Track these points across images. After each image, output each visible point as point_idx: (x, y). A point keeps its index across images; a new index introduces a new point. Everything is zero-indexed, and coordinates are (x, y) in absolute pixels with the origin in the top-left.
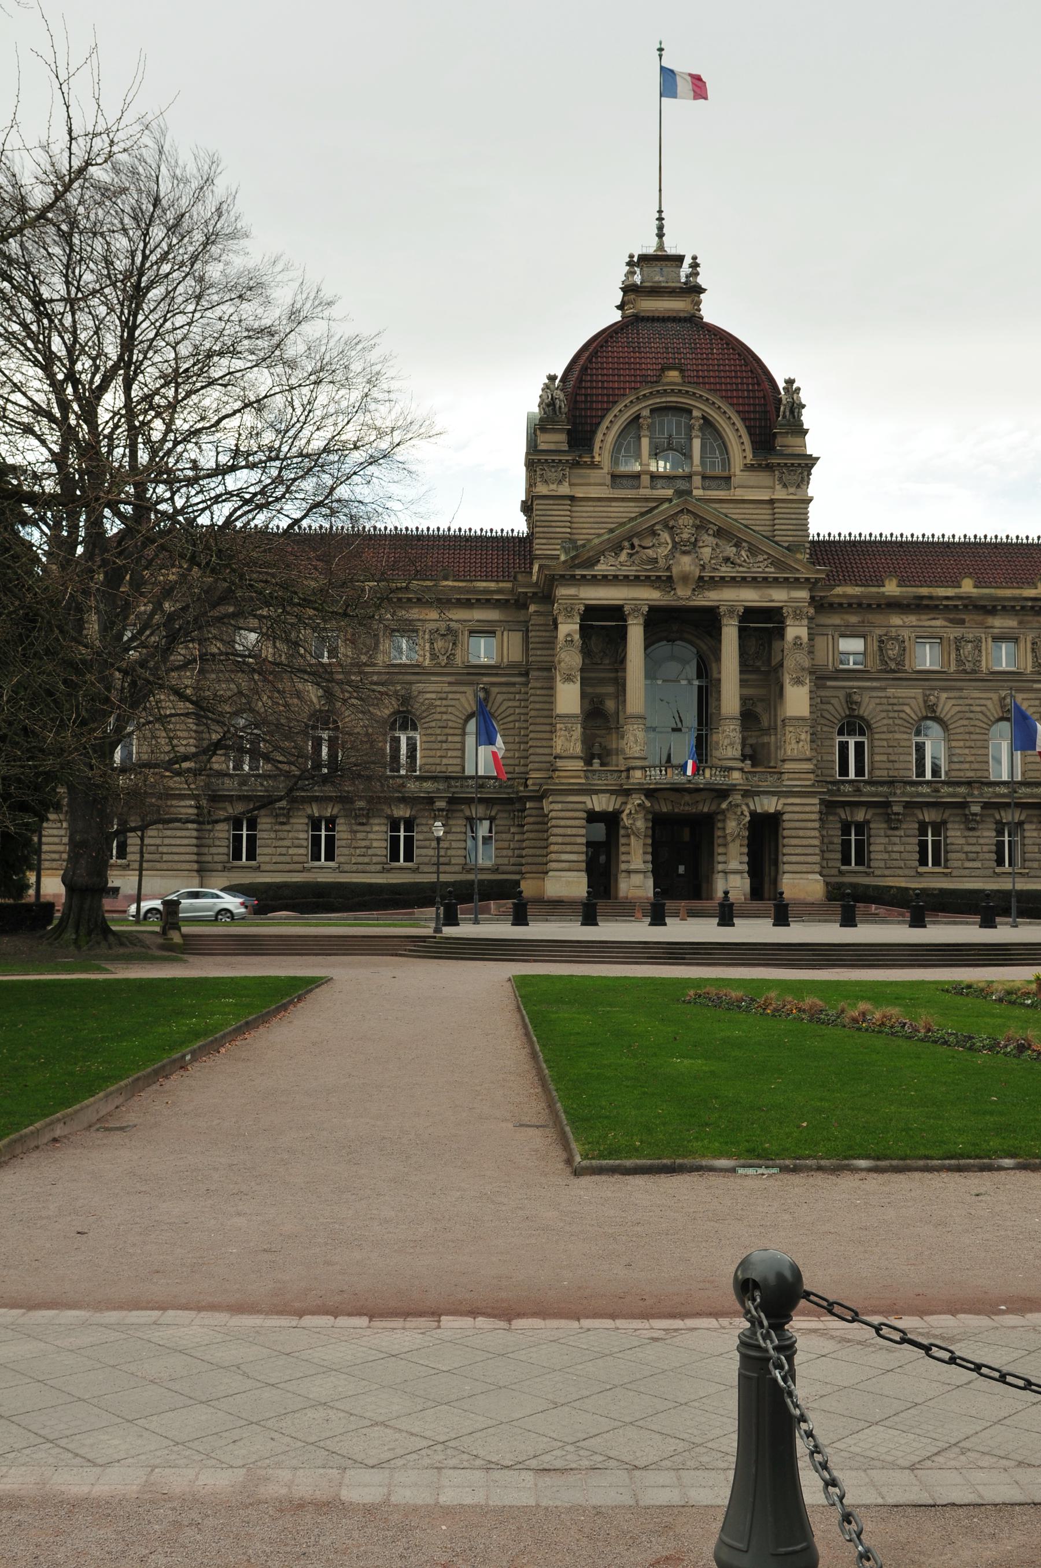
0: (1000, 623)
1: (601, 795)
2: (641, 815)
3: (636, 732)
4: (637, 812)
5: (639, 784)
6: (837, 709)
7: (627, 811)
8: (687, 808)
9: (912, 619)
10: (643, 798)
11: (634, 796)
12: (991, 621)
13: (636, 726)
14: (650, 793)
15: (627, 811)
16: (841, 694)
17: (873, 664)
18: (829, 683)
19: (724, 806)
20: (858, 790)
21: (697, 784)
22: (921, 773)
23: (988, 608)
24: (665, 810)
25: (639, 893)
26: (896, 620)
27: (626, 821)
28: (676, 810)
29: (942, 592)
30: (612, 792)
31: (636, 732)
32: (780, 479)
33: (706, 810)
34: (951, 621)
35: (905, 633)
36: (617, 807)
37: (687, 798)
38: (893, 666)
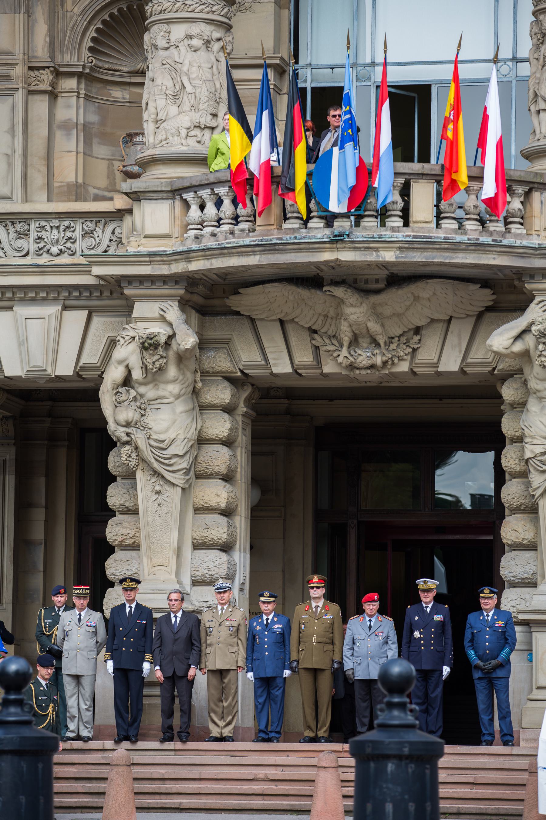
1: (22, 311)
2: (172, 386)
3: (183, 55)
4: (154, 375)
5: (153, 257)
7: (114, 374)
8: (364, 357)
10: (173, 313)
11: (141, 309)
13: (178, 31)
14: (212, 298)
15: (114, 374)
19: (501, 339)
21: (368, 245)
24: (282, 366)
27: (115, 413)
28: (328, 368)
30: (68, 297)
31: (183, 55)
33: (451, 363)
36: (92, 357)
37: (356, 311)
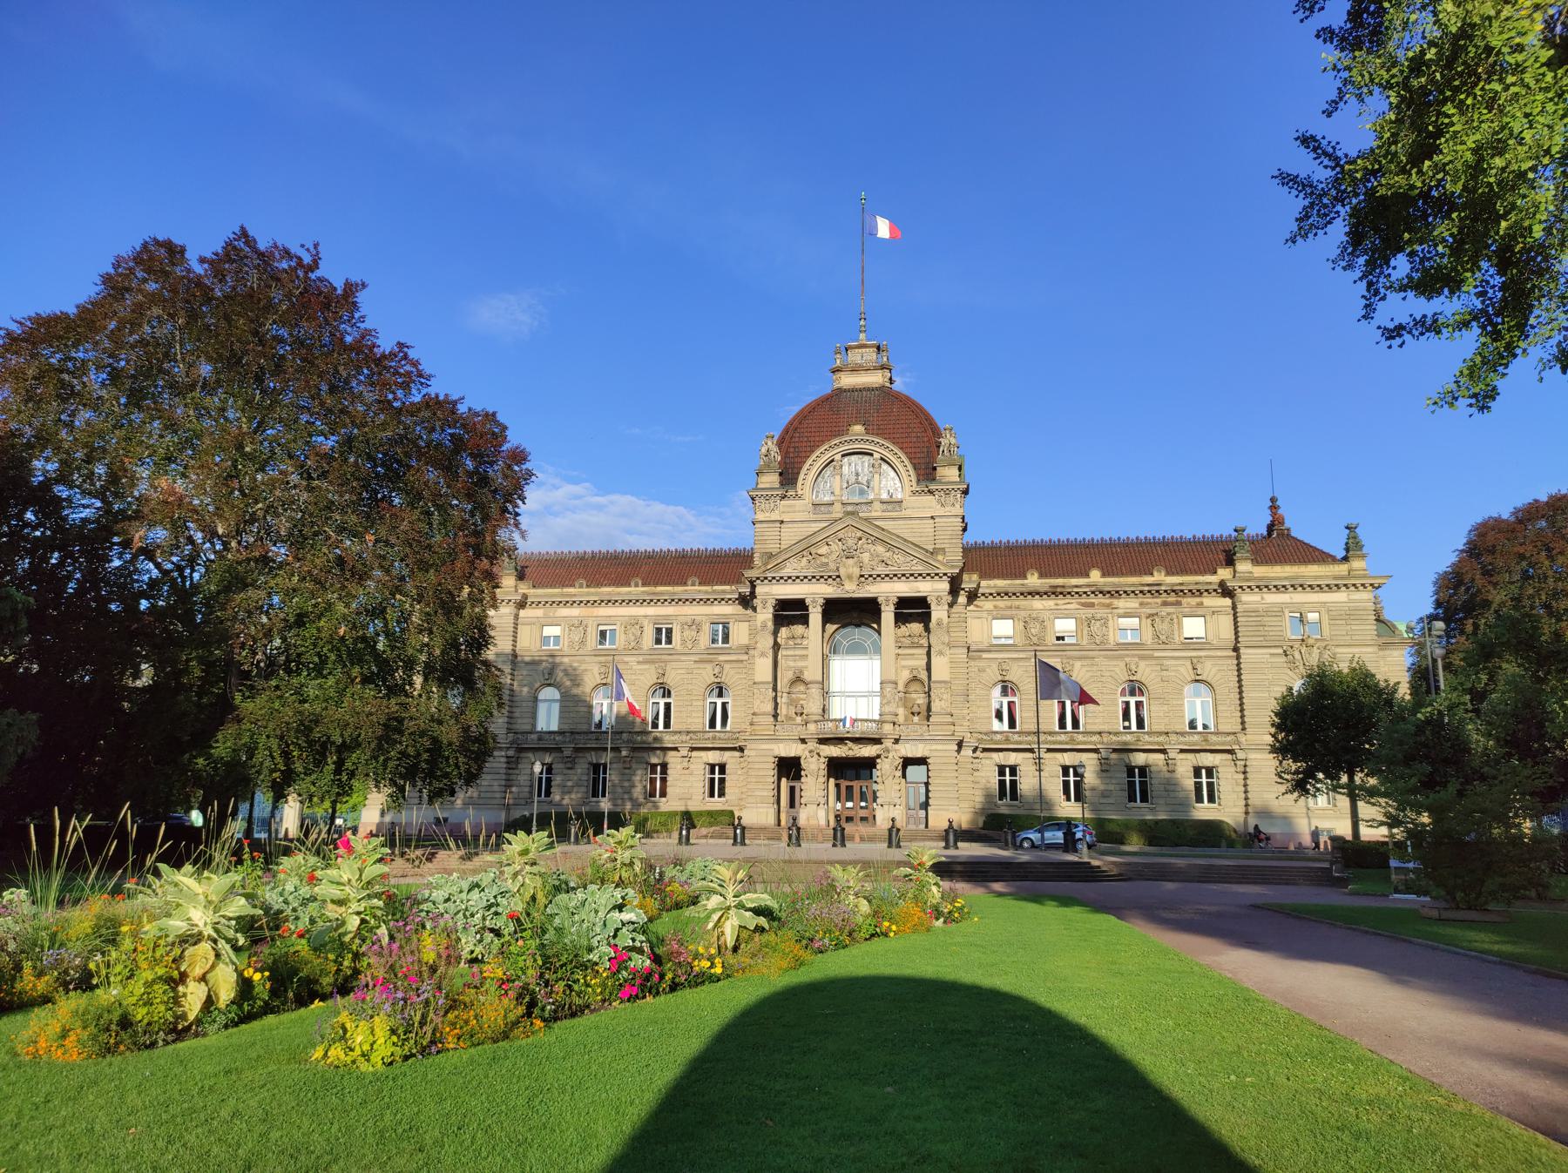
0: (1122, 604)
6: (993, 674)
9: (1050, 603)
12: (1116, 602)
16: (995, 666)
17: (1020, 641)
18: (985, 655)
20: (1007, 740)
22: (1062, 725)
23: (1116, 594)
25: (813, 822)
26: (1037, 603)
29: (1074, 581)
32: (939, 501)
34: (1084, 605)
35: (1046, 615)
38: (1035, 640)
